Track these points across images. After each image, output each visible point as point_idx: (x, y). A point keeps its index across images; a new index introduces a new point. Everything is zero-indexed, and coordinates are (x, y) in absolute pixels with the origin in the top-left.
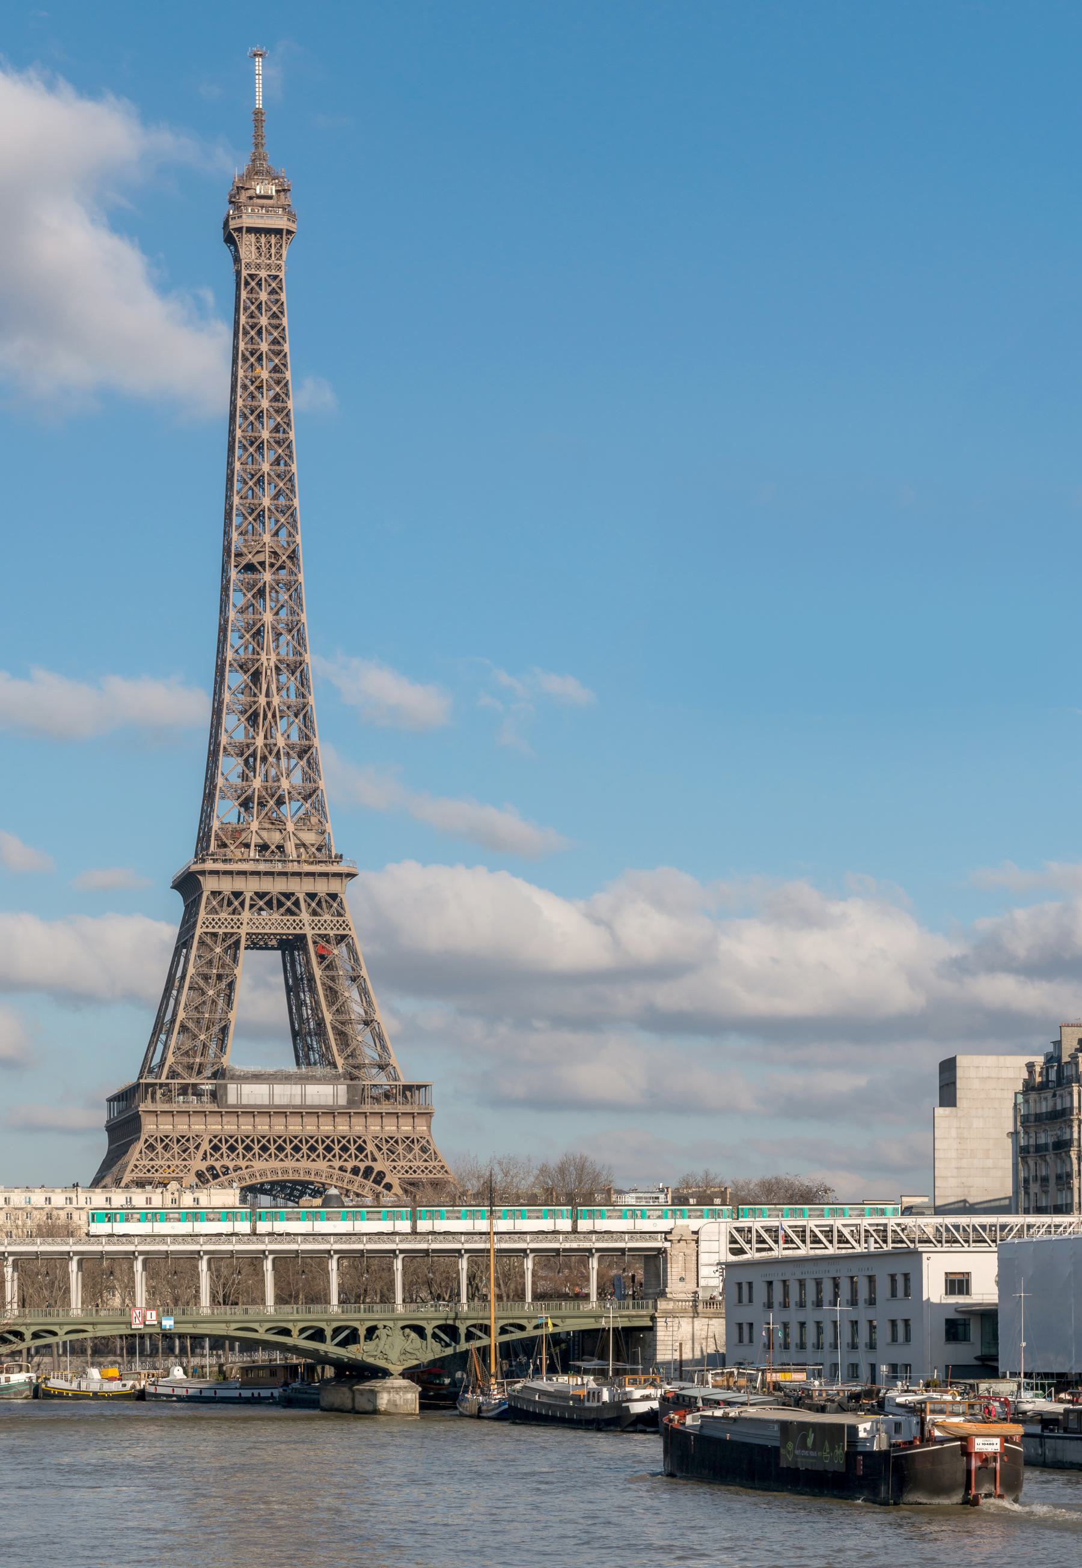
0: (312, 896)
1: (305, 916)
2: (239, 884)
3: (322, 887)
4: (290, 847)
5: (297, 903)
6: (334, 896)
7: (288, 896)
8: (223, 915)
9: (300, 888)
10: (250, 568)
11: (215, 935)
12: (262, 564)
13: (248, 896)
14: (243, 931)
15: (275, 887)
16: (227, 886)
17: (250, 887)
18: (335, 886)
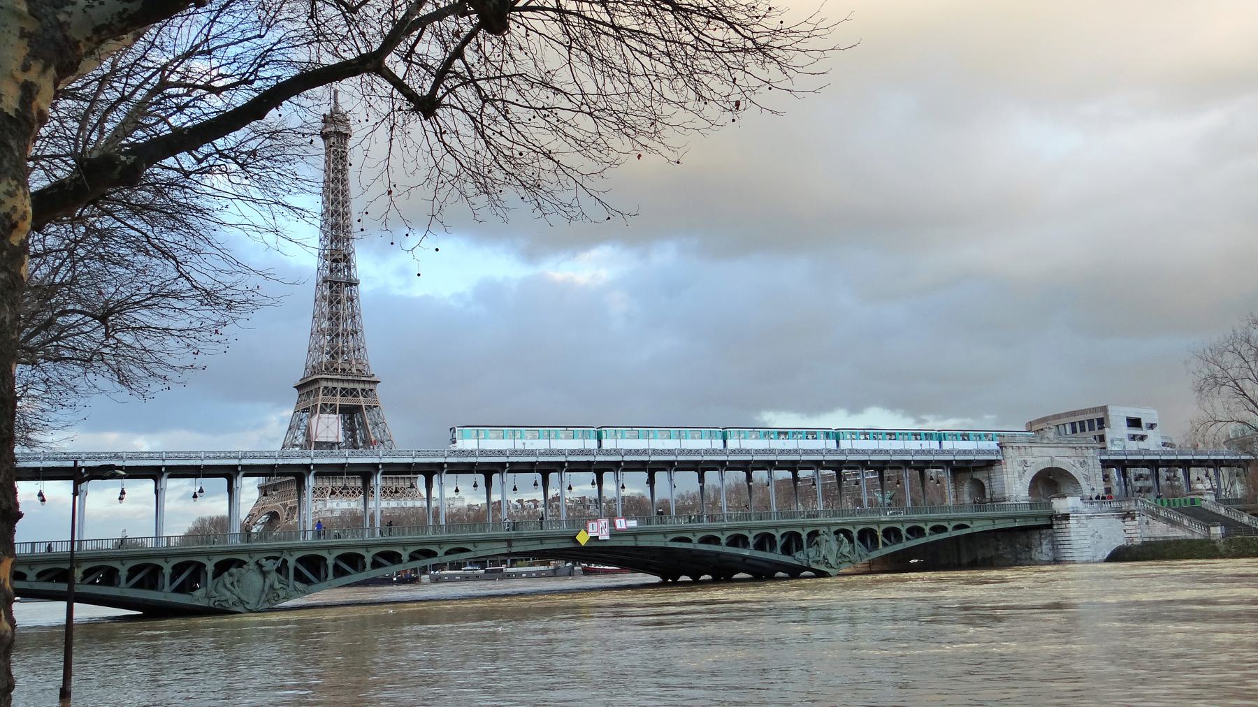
0: (363, 390)
1: (361, 398)
2: (335, 384)
3: (367, 387)
4: (354, 370)
5: (358, 392)
6: (371, 390)
7: (355, 389)
8: (329, 396)
9: (359, 387)
10: (335, 261)
11: (326, 405)
12: (341, 259)
13: (339, 389)
14: (338, 403)
15: (351, 386)
16: (330, 385)
17: (340, 386)
18: (372, 386)
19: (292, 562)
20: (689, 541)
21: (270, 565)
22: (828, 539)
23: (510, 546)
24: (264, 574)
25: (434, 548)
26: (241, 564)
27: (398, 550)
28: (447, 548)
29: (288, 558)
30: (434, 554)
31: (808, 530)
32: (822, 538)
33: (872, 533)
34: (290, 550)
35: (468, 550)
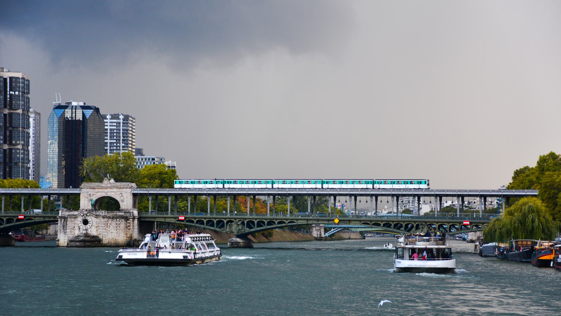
19: (246, 222)
20: (369, 224)
21: (240, 223)
22: (423, 227)
23: (308, 222)
24: (238, 225)
25: (285, 221)
26: (232, 222)
27: (275, 221)
28: (288, 221)
29: (245, 221)
30: (285, 223)
31: (417, 223)
32: (420, 226)
33: (253, 223)
34: (246, 219)
35: (295, 222)
